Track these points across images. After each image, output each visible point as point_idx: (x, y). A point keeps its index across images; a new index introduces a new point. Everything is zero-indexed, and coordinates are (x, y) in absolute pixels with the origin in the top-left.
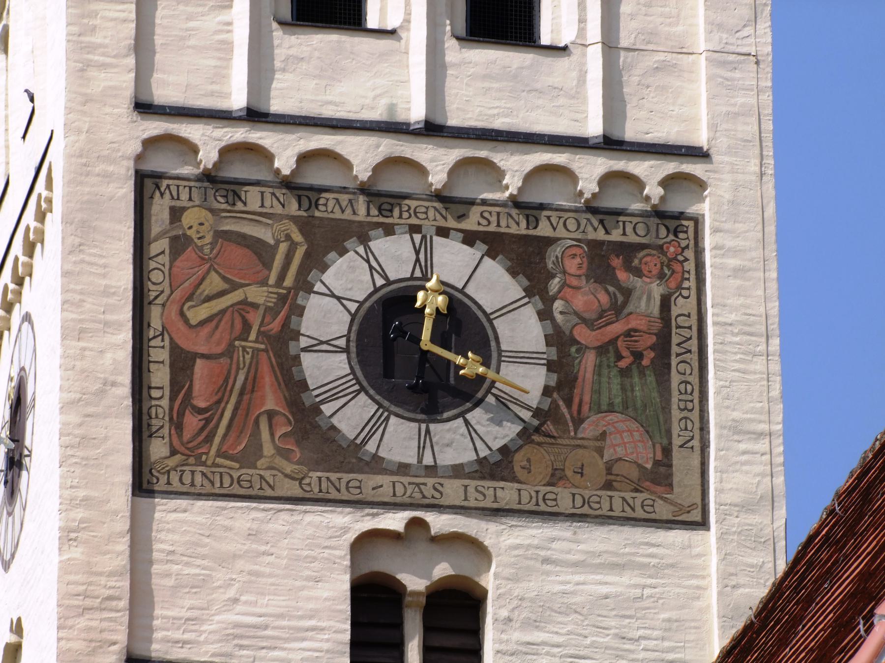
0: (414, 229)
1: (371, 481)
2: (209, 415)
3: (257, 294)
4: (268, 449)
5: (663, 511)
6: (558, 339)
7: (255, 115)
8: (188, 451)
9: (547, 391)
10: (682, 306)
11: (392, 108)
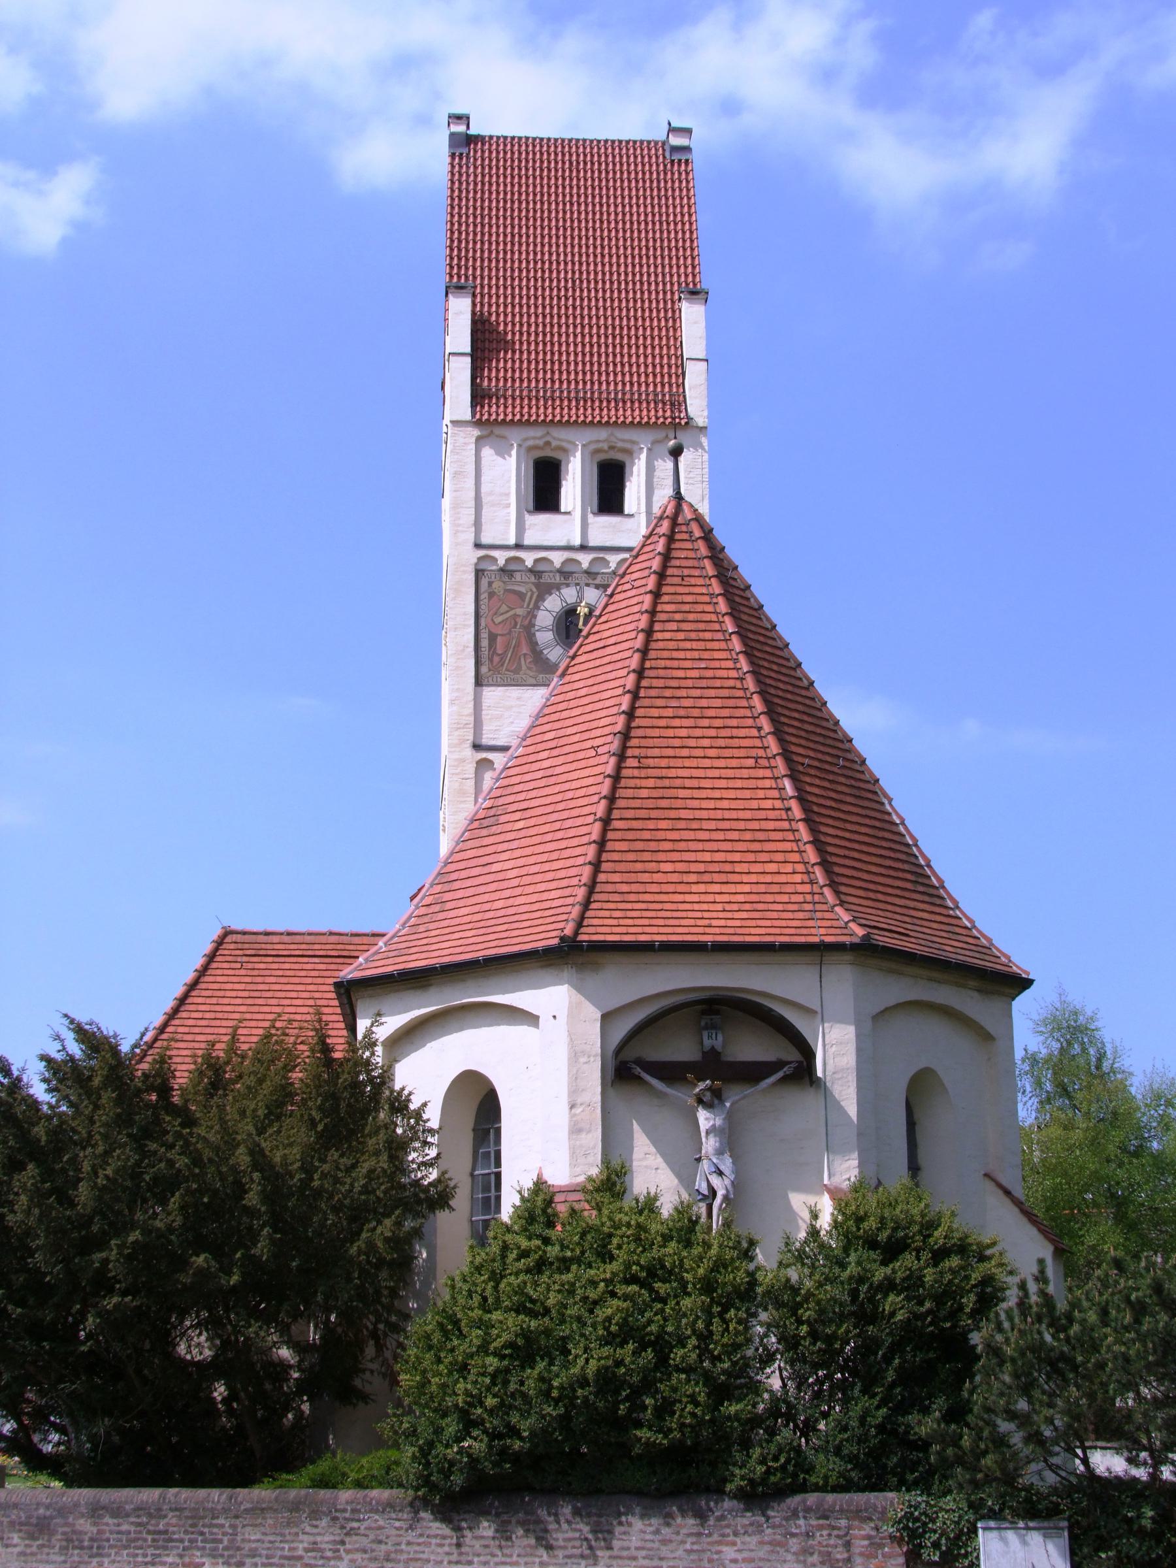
0: (577, 584)
2: (502, 657)
3: (520, 611)
4: (524, 667)
7: (518, 546)
8: (494, 669)
11: (569, 541)
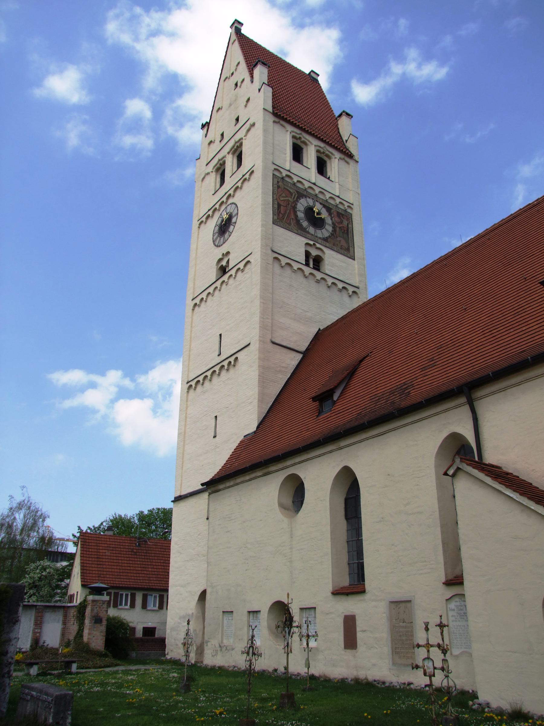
0: (313, 199)
1: (308, 235)
2: (284, 215)
3: (290, 199)
5: (349, 256)
6: (333, 223)
10: (350, 226)
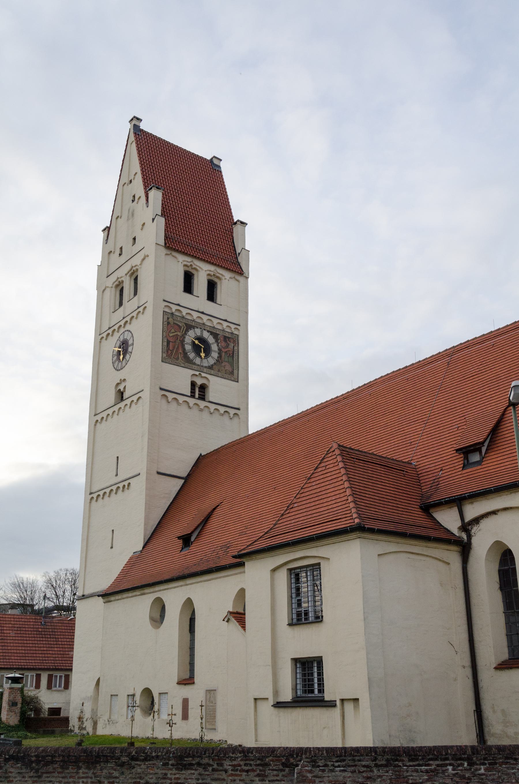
0: (201, 328)
3: (179, 333)
4: (180, 358)
6: (219, 350)
9: (218, 357)
